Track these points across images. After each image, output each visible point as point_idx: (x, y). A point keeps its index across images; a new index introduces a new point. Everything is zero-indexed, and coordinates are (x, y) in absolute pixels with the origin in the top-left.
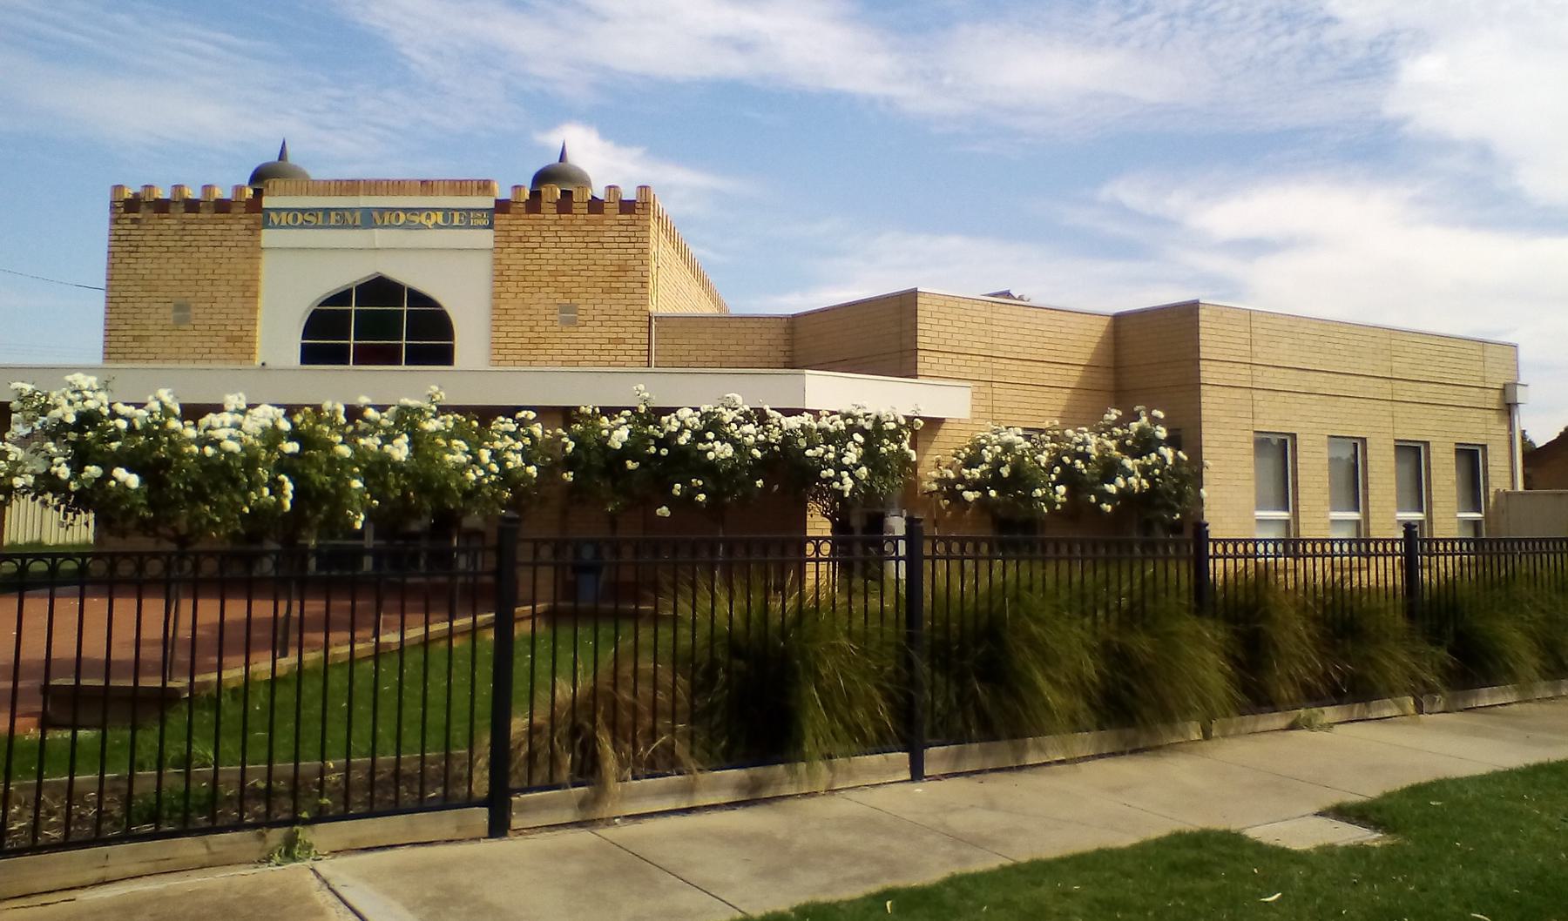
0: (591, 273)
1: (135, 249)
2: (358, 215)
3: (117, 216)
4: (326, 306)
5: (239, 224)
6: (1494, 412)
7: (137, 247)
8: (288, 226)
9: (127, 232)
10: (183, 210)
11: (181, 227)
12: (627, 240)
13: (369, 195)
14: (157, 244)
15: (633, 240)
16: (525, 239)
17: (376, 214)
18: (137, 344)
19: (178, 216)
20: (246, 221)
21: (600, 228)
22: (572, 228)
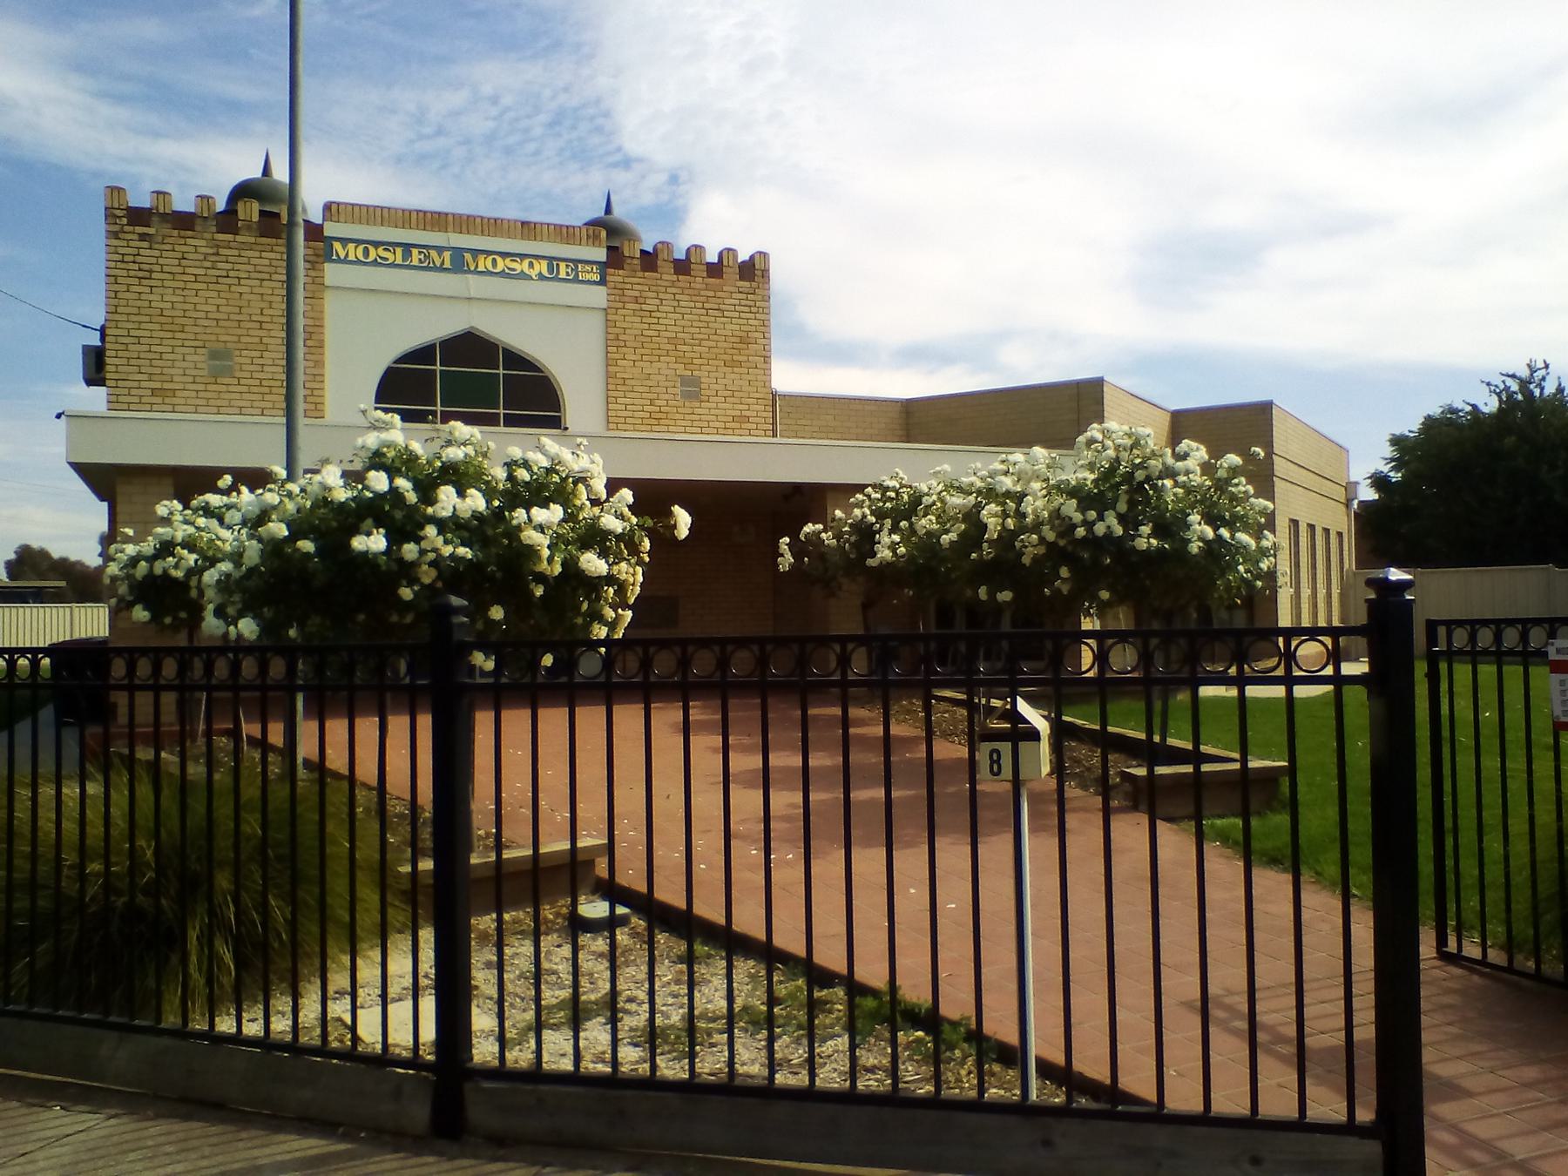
0: (713, 344)
1: (147, 274)
2: (447, 255)
3: (116, 228)
4: (401, 363)
6: (1341, 505)
7: (151, 271)
8: (358, 262)
9: (135, 252)
10: (214, 229)
11: (214, 251)
12: (747, 309)
14: (180, 270)
16: (642, 300)
17: (468, 256)
18: (159, 400)
21: (719, 294)
22: (690, 292)
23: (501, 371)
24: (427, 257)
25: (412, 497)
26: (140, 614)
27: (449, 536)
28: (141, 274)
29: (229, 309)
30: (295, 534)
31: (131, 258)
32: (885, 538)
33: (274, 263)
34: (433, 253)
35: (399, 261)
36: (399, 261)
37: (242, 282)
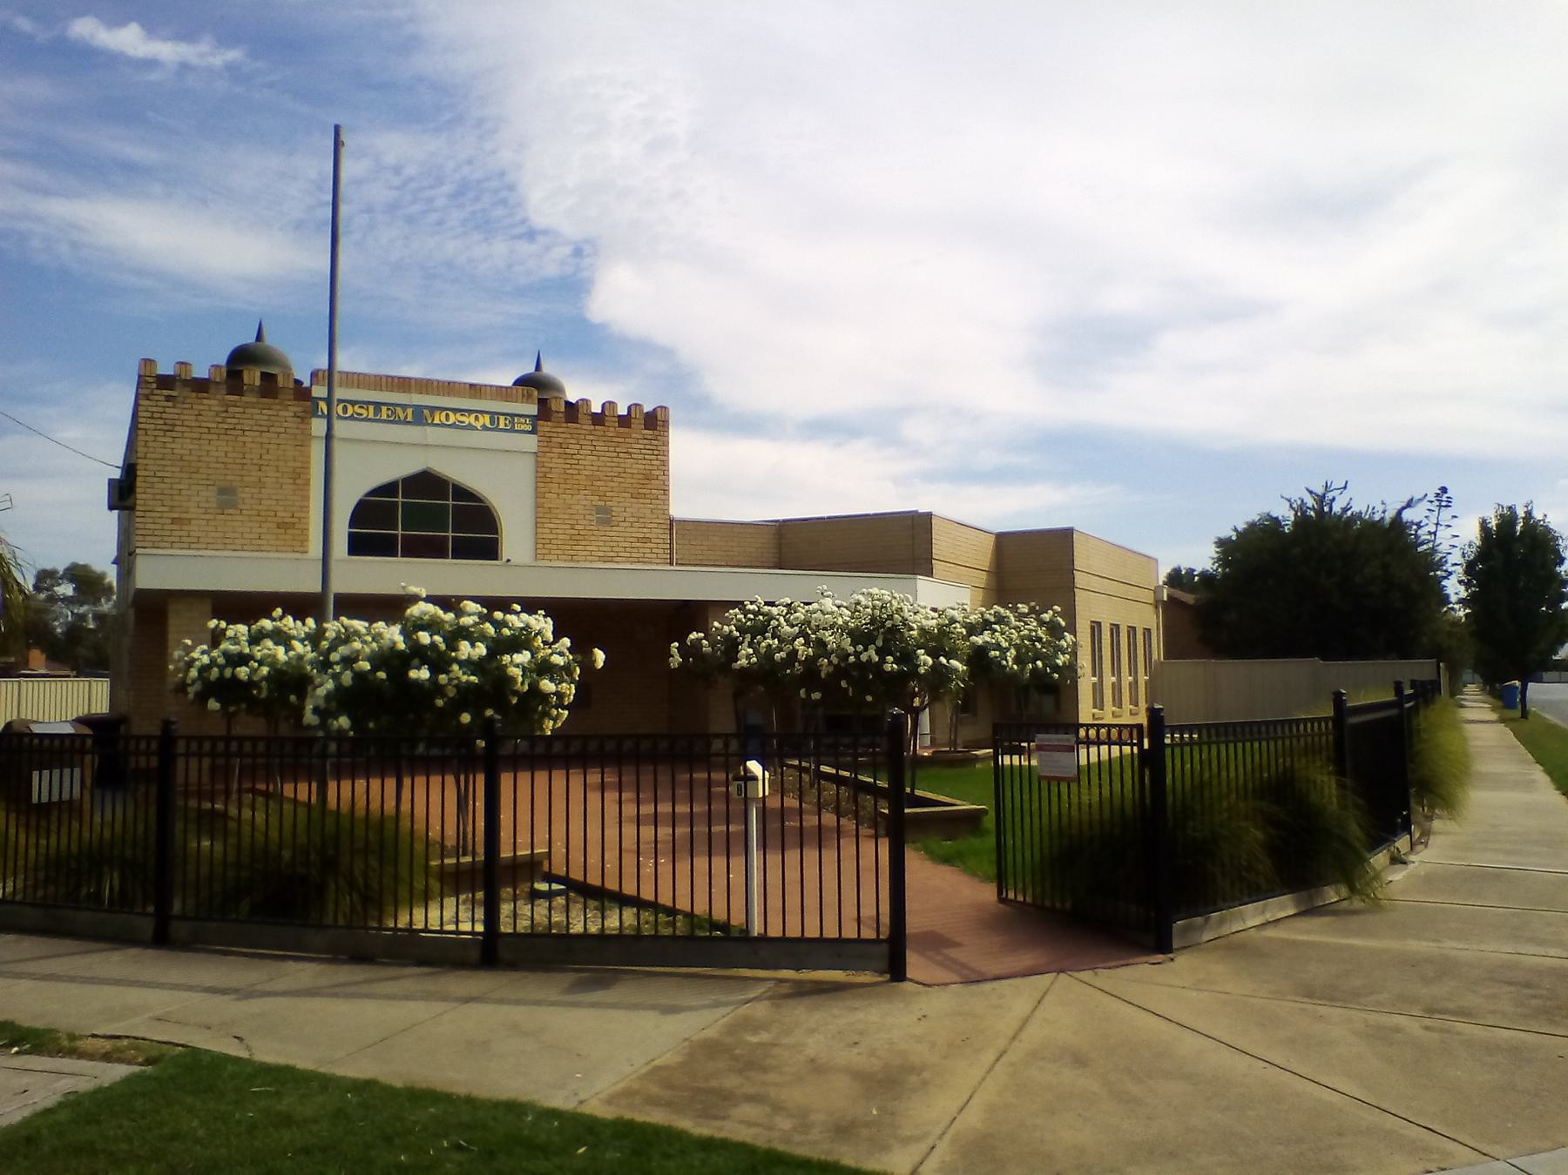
0: (623, 480)
1: (171, 428)
2: (410, 411)
5: (287, 410)
9: (161, 410)
10: (224, 392)
12: (650, 452)
13: (421, 393)
14: (197, 424)
15: (656, 452)
17: (426, 412)
19: (219, 397)
20: (295, 409)
22: (604, 439)
23: (451, 502)
24: (394, 413)
25: (443, 647)
26: (213, 705)
27: (465, 670)
28: (166, 428)
29: (235, 455)
30: (375, 669)
31: (159, 415)
32: (745, 650)
33: (272, 418)
34: (399, 410)
35: (371, 415)
36: (371, 415)
37: (246, 433)
